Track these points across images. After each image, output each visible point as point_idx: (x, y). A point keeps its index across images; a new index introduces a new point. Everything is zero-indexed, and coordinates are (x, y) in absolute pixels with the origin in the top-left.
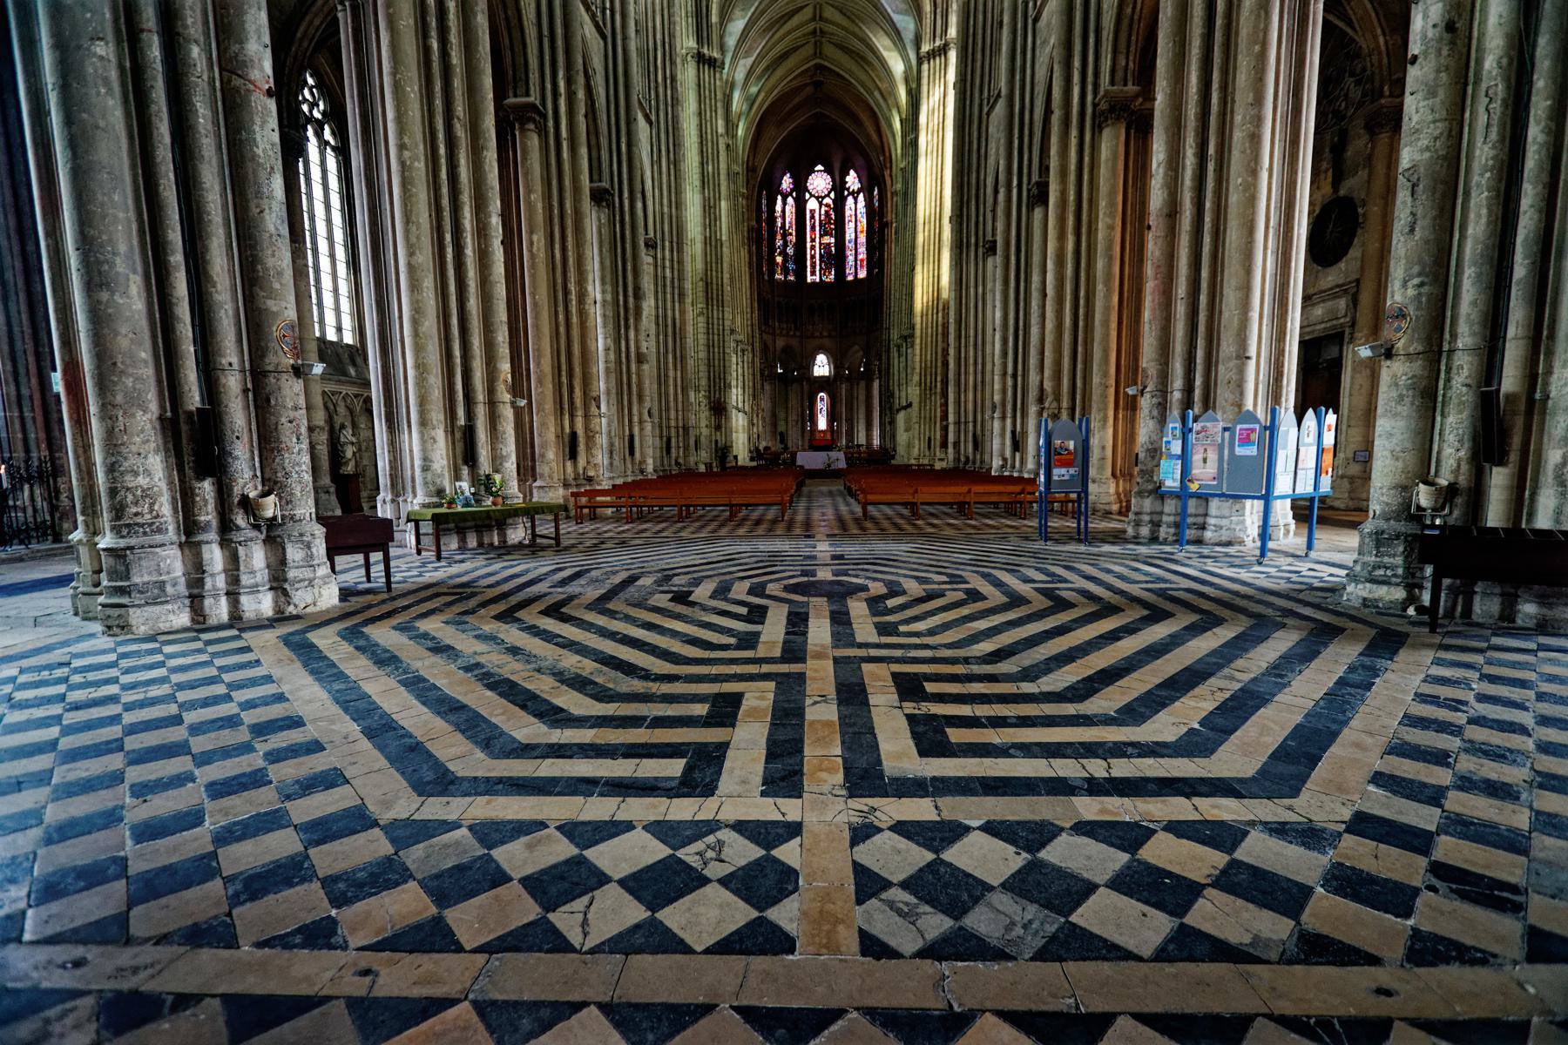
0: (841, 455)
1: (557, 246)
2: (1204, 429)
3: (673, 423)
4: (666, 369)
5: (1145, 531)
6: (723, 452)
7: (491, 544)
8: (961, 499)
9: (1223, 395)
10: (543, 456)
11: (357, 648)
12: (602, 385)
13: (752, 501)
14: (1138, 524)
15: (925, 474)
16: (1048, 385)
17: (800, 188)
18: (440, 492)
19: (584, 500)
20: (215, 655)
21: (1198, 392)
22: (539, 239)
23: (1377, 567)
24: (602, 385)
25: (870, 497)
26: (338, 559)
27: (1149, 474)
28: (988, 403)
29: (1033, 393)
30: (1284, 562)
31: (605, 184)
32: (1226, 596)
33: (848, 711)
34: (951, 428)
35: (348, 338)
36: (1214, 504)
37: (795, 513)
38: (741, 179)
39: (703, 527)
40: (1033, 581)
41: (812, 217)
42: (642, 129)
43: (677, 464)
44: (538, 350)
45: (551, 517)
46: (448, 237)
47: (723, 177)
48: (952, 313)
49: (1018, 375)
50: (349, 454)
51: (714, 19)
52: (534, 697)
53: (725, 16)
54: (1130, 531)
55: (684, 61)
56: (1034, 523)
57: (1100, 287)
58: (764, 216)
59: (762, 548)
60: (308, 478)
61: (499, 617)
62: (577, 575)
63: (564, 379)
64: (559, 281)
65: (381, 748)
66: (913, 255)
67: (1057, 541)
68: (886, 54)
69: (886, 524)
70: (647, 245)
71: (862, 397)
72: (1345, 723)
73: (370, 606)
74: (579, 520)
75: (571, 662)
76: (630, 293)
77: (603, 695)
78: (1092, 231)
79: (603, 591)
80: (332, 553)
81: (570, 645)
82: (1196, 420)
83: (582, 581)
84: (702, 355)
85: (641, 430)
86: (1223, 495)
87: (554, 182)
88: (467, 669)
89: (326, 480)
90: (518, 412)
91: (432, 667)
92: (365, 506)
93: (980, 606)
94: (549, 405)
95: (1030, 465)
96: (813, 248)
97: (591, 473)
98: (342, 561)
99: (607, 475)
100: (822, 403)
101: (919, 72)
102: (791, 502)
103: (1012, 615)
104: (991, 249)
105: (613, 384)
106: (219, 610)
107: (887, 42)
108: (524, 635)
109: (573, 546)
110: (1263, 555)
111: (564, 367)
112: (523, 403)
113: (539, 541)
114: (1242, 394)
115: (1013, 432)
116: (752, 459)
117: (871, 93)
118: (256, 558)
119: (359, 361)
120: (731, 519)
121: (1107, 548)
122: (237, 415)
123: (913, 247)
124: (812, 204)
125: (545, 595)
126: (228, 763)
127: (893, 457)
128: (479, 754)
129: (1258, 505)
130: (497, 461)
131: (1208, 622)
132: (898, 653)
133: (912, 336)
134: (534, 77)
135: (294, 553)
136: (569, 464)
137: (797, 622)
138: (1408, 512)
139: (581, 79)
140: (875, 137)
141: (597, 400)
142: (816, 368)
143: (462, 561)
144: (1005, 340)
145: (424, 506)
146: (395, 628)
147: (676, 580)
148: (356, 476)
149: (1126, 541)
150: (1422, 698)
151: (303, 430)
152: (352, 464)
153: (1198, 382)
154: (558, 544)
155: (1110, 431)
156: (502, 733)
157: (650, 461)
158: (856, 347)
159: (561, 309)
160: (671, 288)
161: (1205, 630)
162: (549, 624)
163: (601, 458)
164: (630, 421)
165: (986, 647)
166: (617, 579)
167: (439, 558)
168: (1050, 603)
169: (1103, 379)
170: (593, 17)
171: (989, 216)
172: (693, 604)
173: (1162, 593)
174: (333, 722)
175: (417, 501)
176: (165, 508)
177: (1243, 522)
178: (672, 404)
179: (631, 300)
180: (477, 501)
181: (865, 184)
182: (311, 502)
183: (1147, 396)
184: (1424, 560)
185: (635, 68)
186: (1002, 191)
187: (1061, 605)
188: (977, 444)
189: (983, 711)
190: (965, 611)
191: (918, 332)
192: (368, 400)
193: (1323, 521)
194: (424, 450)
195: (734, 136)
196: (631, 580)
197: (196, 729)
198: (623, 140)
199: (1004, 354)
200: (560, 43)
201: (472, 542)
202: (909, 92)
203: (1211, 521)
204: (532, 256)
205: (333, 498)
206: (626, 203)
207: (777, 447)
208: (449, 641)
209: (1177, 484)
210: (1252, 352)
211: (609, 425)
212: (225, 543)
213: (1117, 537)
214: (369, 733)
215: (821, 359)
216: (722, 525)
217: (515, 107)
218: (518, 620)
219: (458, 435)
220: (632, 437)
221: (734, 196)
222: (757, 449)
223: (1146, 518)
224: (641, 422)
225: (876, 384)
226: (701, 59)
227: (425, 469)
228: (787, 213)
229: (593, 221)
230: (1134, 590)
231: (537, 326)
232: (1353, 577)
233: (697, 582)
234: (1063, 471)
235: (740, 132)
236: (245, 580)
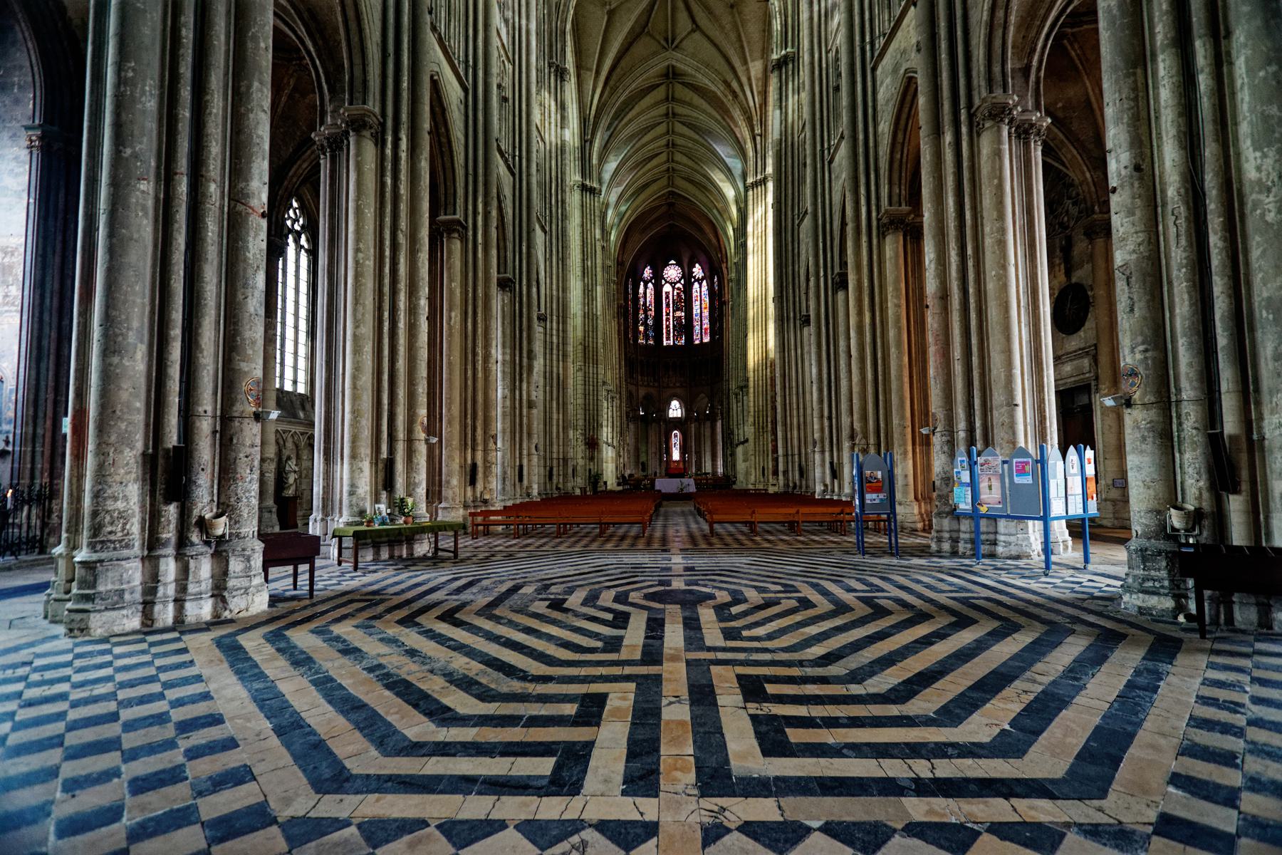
0: (692, 481)
1: (470, 320)
2: (986, 462)
3: (555, 456)
4: (551, 413)
5: (946, 546)
6: (595, 478)
7: (400, 557)
8: (791, 519)
9: (999, 434)
10: (448, 482)
11: (278, 650)
12: (499, 425)
13: (616, 519)
14: (939, 540)
15: (761, 497)
16: (857, 426)
17: (658, 279)
18: (362, 513)
19: (480, 519)
20: (156, 656)
21: (978, 433)
22: (456, 316)
23: (1145, 579)
24: (499, 425)
25: (716, 517)
26: (271, 570)
27: (945, 498)
28: (810, 439)
29: (845, 433)
30: (1066, 573)
31: (509, 275)
32: (1021, 605)
33: (699, 710)
34: (781, 459)
35: (301, 389)
36: (1002, 524)
37: (653, 530)
38: (613, 270)
39: (576, 542)
40: (855, 591)
41: (667, 297)
42: (539, 236)
43: (558, 488)
44: (450, 399)
45: (452, 533)
46: (386, 314)
47: (599, 269)
48: (778, 370)
49: (832, 418)
50: (291, 480)
51: (595, 161)
52: (425, 696)
53: (602, 159)
54: (934, 547)
55: (572, 189)
56: (853, 539)
57: (893, 350)
58: (630, 297)
59: (626, 560)
60: (255, 502)
61: (401, 622)
62: (470, 584)
63: (469, 421)
64: (470, 345)
65: (288, 745)
66: (746, 325)
67: (873, 555)
68: (721, 184)
69: (729, 540)
70: (539, 319)
71: (708, 433)
72: (1139, 724)
73: (294, 612)
74: (475, 535)
75: (460, 663)
76: (525, 355)
77: (485, 695)
78: (883, 310)
79: (491, 599)
80: (266, 565)
81: (460, 648)
82: (979, 454)
83: (474, 589)
84: (580, 401)
85: (529, 461)
86: (1008, 517)
87: (471, 274)
88: (370, 670)
89: (270, 502)
90: (430, 448)
91: (341, 667)
92: (300, 523)
93: (811, 613)
94: (456, 442)
95: (847, 490)
96: (668, 320)
97: (487, 497)
98: (274, 572)
99: (500, 497)
100: (676, 438)
101: (746, 196)
102: (651, 521)
103: (838, 622)
104: (806, 321)
105: (508, 425)
106: (165, 615)
107: (722, 176)
108: (422, 639)
109: (468, 558)
110: (1048, 567)
111: (469, 412)
112: (434, 440)
113: (440, 553)
114: (1014, 433)
115: (832, 463)
116: (619, 484)
117: (710, 210)
118: (204, 569)
119: (308, 406)
120: (600, 535)
121: (916, 561)
122: (205, 452)
123: (746, 319)
124: (667, 288)
125: (442, 602)
126: (152, 759)
127: (734, 483)
128: (374, 752)
129: (1039, 525)
130: (410, 488)
131: (1006, 629)
132: (741, 656)
133: (747, 386)
135: (235, 565)
136: (469, 489)
137: (655, 627)
138: (1163, 531)
139: (495, 203)
140: (714, 241)
141: (495, 437)
142: (671, 411)
143: (375, 571)
144: (820, 390)
145: (348, 524)
146: (312, 632)
147: (553, 589)
148: (295, 498)
149: (931, 555)
150: (1204, 700)
151: (256, 463)
152: (293, 488)
153: (978, 424)
154: (456, 556)
155: (911, 462)
156: (396, 732)
157: (535, 486)
158: (703, 395)
159: (470, 367)
160: (558, 350)
161: (1006, 635)
162: (444, 628)
163: (495, 484)
164: (521, 454)
165: (817, 651)
166: (504, 588)
167: (356, 569)
168: (869, 610)
169: (901, 420)
170: (506, 161)
171: (803, 297)
172: (567, 610)
173: (964, 601)
174: (249, 720)
175: (341, 520)
176: (135, 528)
177: (1028, 539)
178: (555, 440)
179: (525, 360)
180: (392, 520)
181: (708, 274)
182: (255, 522)
183: (938, 435)
184: (1185, 574)
186: (812, 279)
187: (880, 612)
188: (802, 473)
189: (818, 711)
190: (798, 618)
191: (751, 384)
192: (312, 437)
193: (1096, 538)
194: (352, 478)
195: (608, 241)
196: (515, 589)
197: (130, 726)
198: (524, 244)
199: (821, 401)
200: (481, 179)
201: (385, 554)
202: (739, 210)
203: (1001, 538)
204: (450, 328)
205: (275, 516)
206: (524, 288)
207: (639, 474)
208: (357, 644)
209: (969, 507)
210: (1019, 400)
211: (503, 457)
212: (180, 556)
213: (923, 551)
214: (279, 731)
215: (675, 404)
216: (593, 540)
218: (418, 624)
219: (381, 466)
220: (521, 467)
221: (607, 283)
222: (623, 476)
223: (947, 535)
224: (529, 455)
225: (719, 424)
226: (584, 188)
227: (352, 493)
228: (648, 295)
229: (498, 302)
230: (942, 598)
231: (450, 380)
232: (1127, 588)
233: (570, 591)
234: (874, 496)
235: (612, 238)
236: (192, 588)
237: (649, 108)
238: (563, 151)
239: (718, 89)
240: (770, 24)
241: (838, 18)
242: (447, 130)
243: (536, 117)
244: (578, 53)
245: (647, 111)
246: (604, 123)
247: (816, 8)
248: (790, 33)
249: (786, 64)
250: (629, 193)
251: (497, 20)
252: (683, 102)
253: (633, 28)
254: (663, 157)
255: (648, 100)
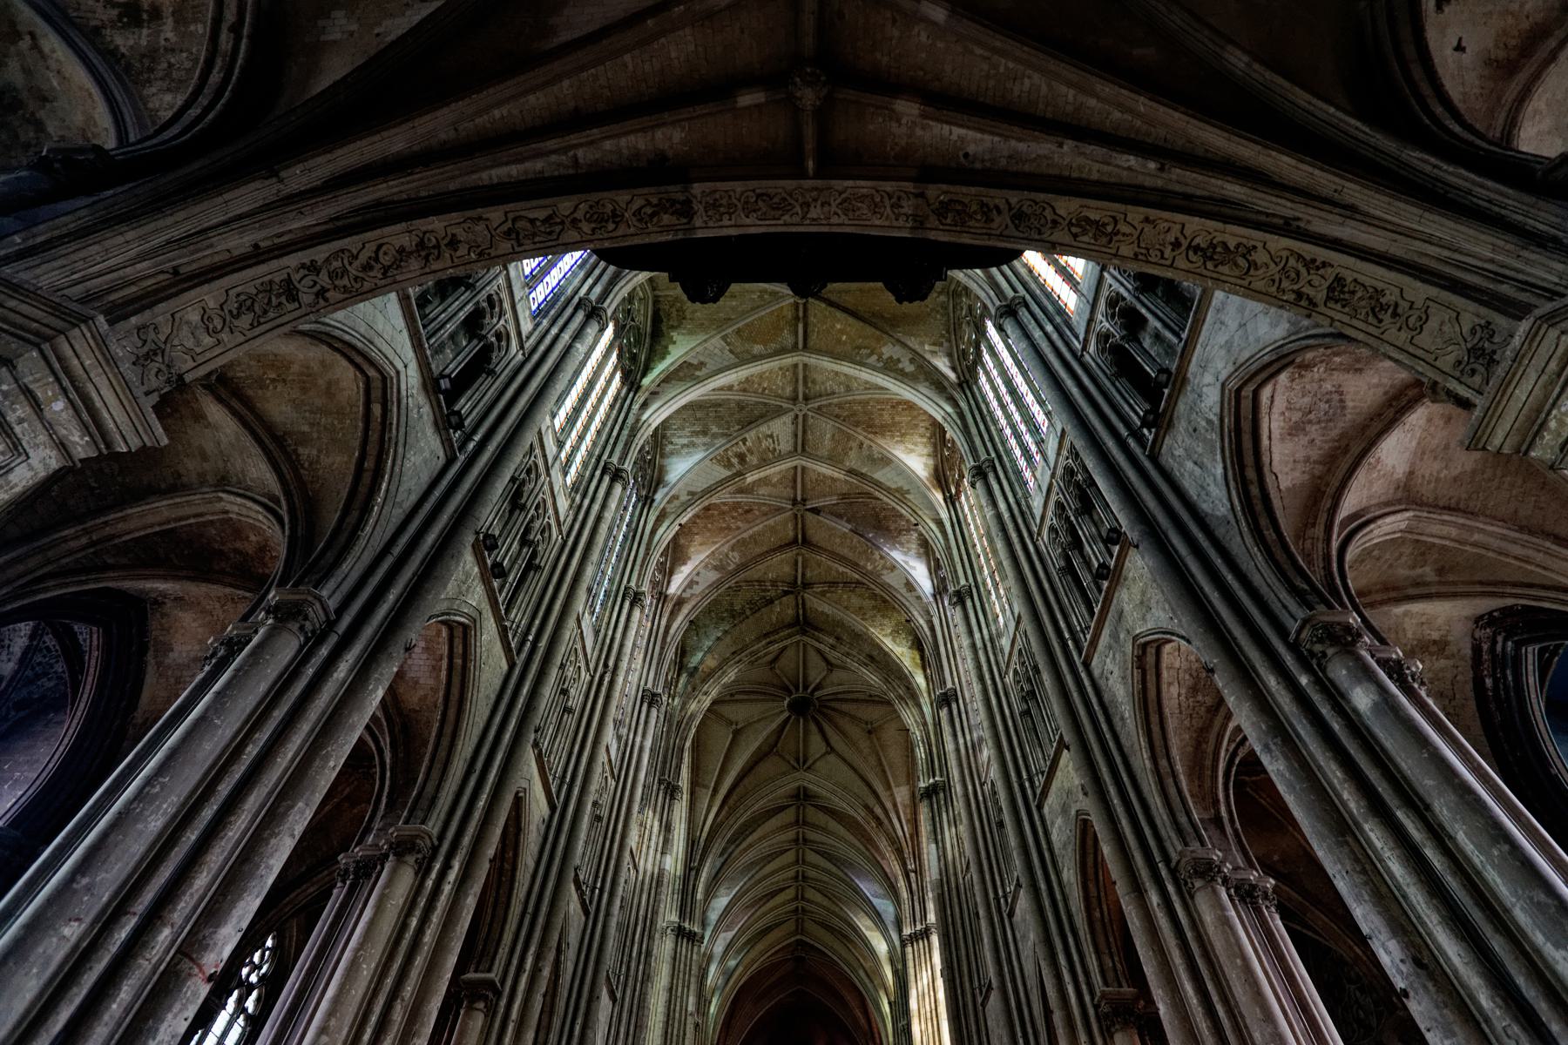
51: (699, 896)
53: (710, 893)
55: (664, 932)
68: (868, 933)
101: (904, 954)
107: (869, 923)
134: (503, 952)
139: (551, 956)
170: (581, 895)
185: (611, 944)
198: (579, 1021)
200: (541, 920)
217: (471, 983)
226: (680, 932)
237: (773, 832)
238: (659, 883)
239: (859, 815)
240: (913, 751)
241: (987, 753)
242: (516, 855)
243: (633, 840)
244: (696, 769)
245: (773, 834)
246: (717, 847)
247: (961, 741)
248: (936, 761)
249: (937, 794)
250: (743, 940)
251: (609, 736)
252: (815, 827)
253: (759, 748)
254: (790, 893)
255: (774, 822)
